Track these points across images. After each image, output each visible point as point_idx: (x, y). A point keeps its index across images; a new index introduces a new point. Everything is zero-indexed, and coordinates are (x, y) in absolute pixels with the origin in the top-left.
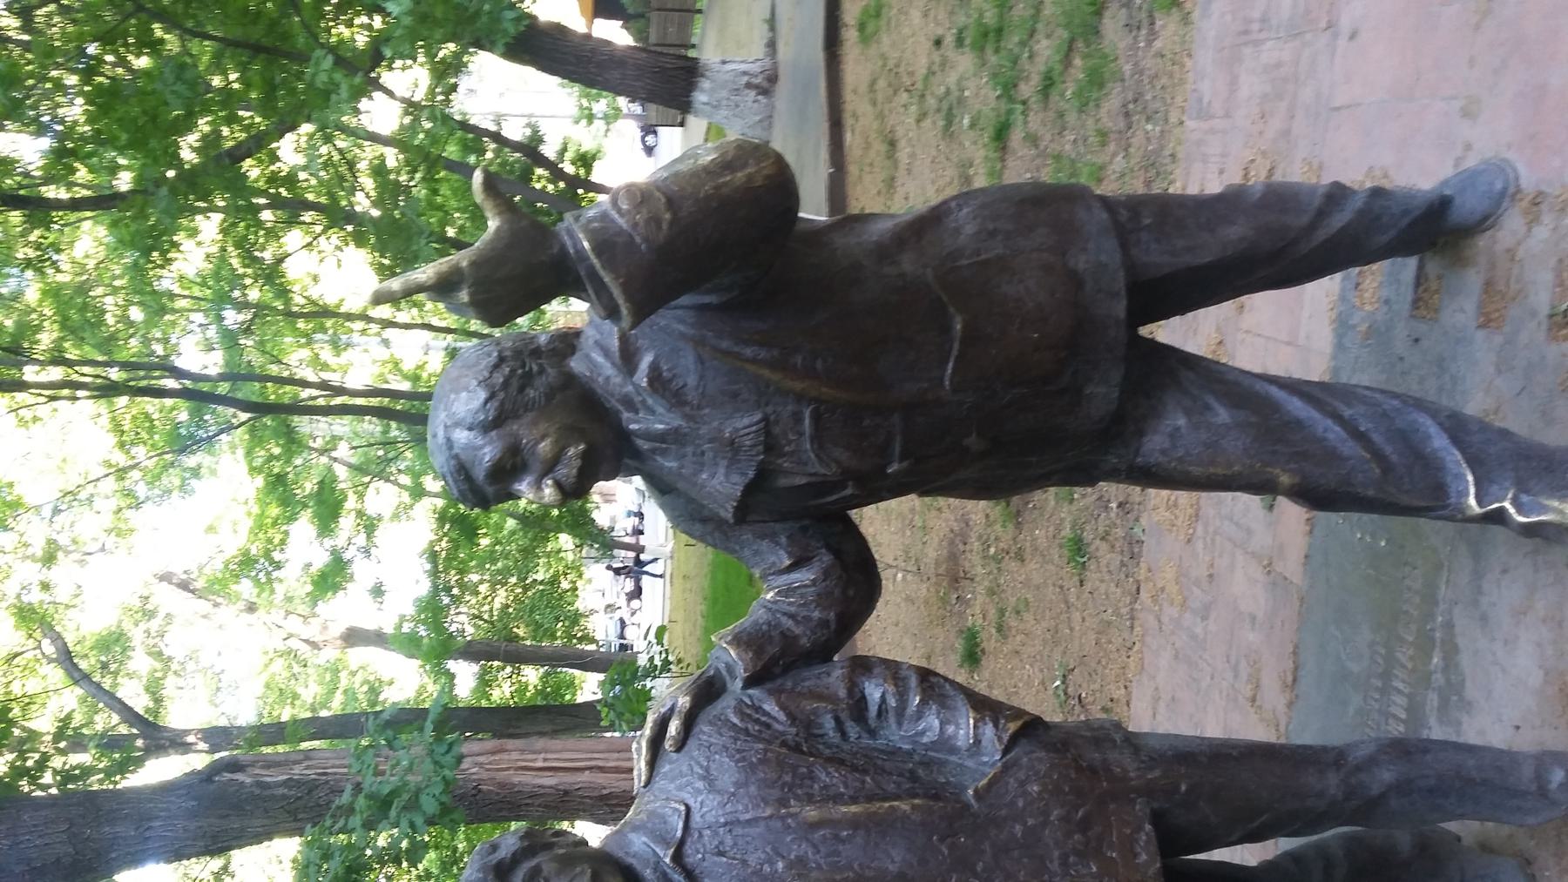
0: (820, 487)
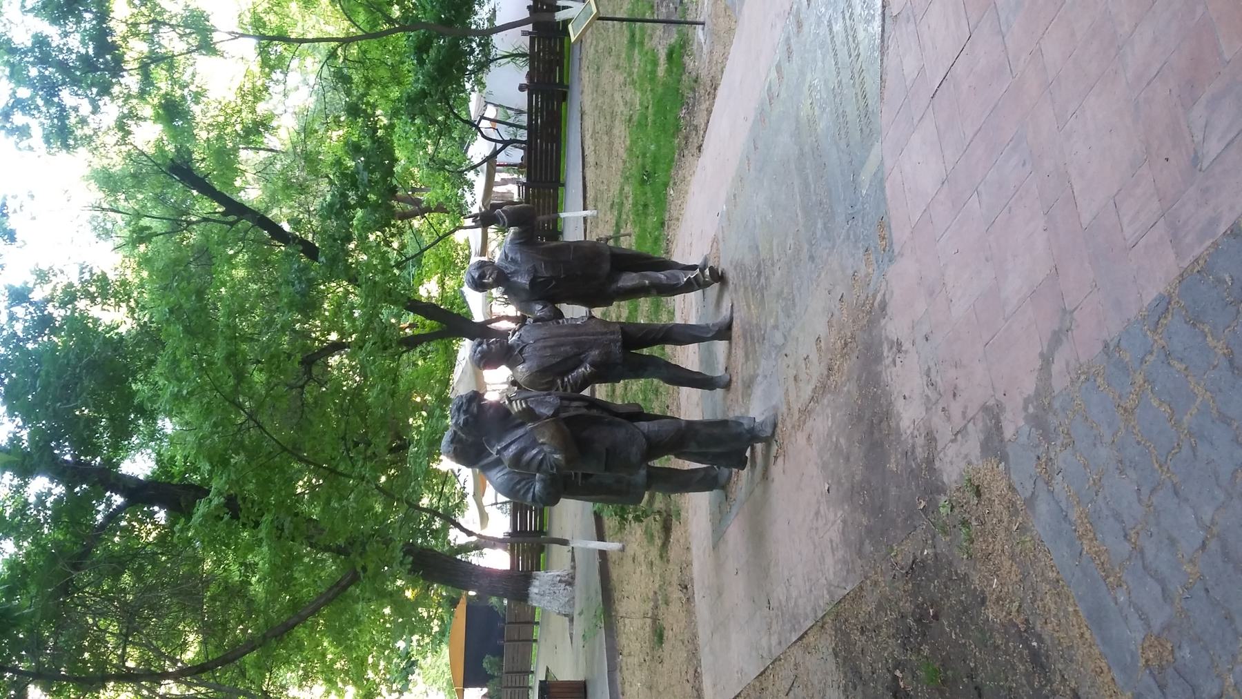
0: (548, 281)
